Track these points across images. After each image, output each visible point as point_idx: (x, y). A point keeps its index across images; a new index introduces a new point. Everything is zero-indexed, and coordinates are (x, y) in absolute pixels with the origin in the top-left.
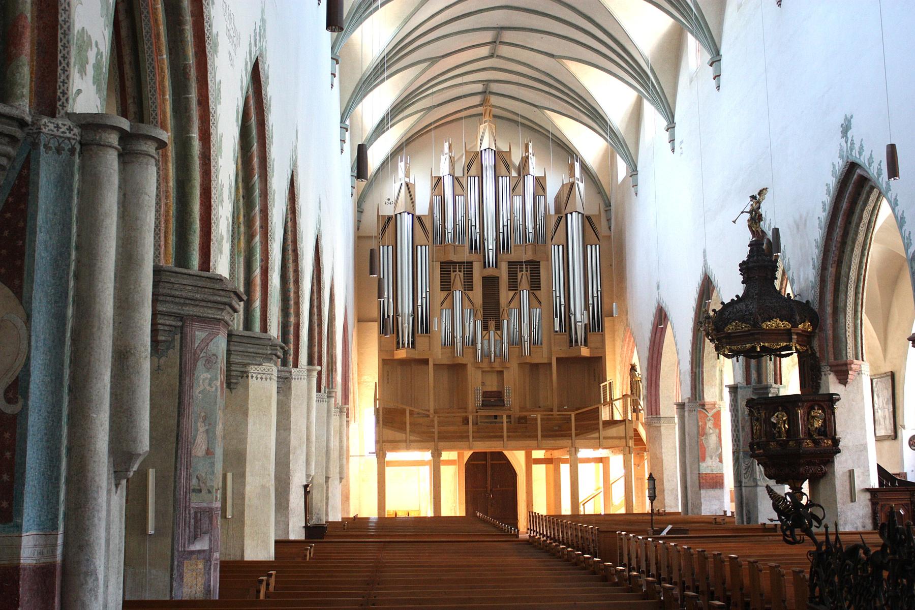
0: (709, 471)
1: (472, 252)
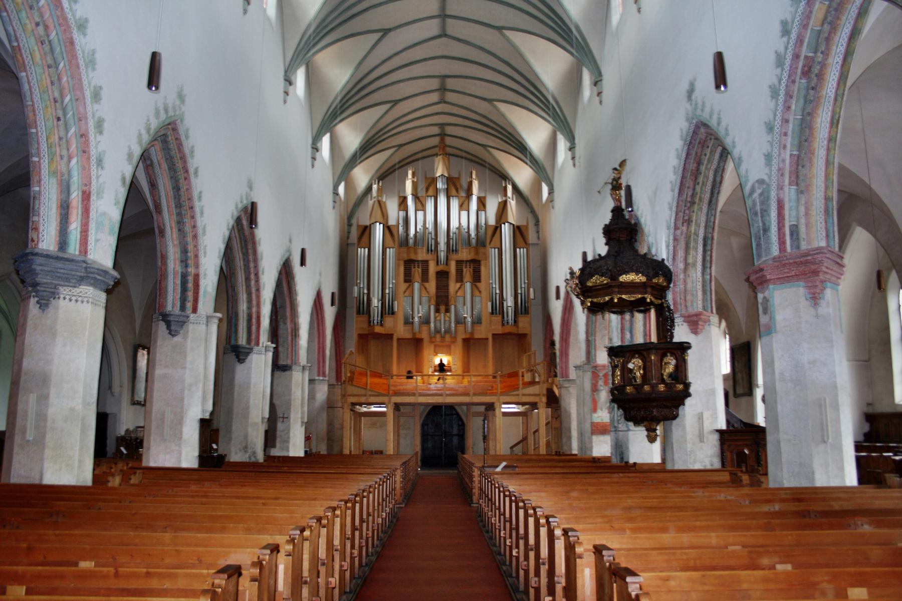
0: (599, 420)
1: (428, 253)
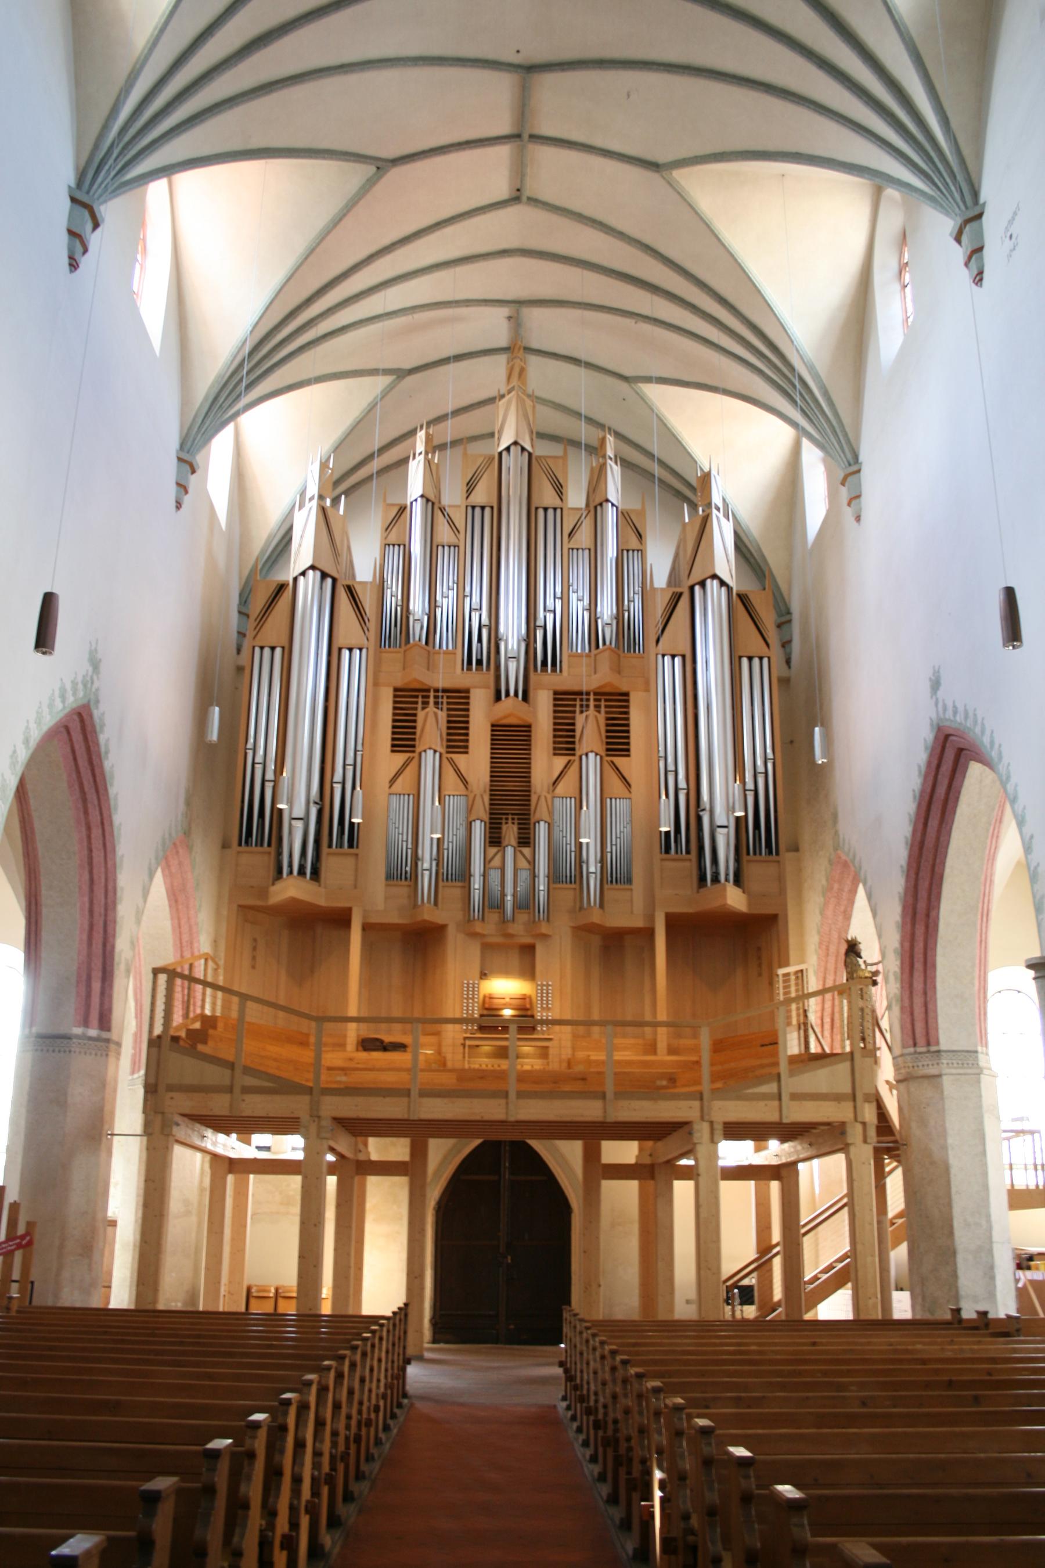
1: (469, 668)
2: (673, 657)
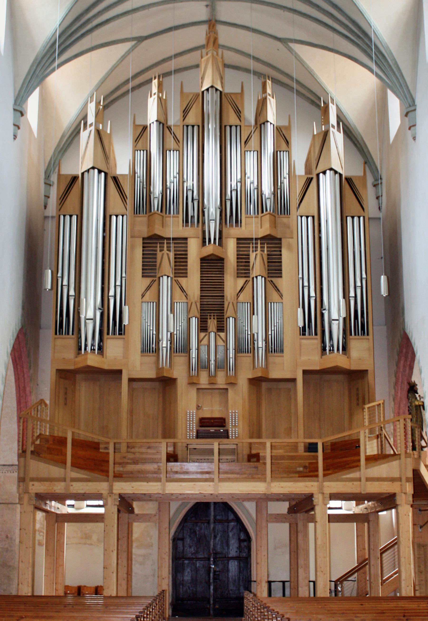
2: (307, 217)
